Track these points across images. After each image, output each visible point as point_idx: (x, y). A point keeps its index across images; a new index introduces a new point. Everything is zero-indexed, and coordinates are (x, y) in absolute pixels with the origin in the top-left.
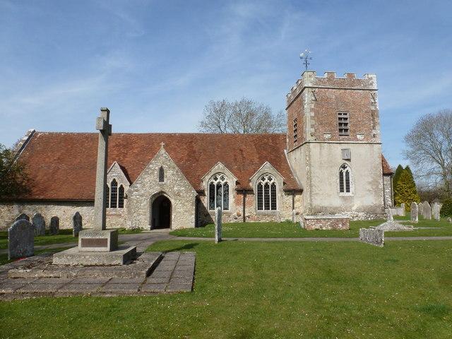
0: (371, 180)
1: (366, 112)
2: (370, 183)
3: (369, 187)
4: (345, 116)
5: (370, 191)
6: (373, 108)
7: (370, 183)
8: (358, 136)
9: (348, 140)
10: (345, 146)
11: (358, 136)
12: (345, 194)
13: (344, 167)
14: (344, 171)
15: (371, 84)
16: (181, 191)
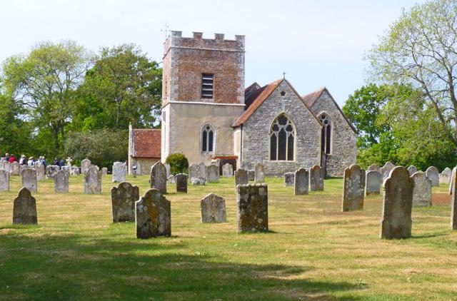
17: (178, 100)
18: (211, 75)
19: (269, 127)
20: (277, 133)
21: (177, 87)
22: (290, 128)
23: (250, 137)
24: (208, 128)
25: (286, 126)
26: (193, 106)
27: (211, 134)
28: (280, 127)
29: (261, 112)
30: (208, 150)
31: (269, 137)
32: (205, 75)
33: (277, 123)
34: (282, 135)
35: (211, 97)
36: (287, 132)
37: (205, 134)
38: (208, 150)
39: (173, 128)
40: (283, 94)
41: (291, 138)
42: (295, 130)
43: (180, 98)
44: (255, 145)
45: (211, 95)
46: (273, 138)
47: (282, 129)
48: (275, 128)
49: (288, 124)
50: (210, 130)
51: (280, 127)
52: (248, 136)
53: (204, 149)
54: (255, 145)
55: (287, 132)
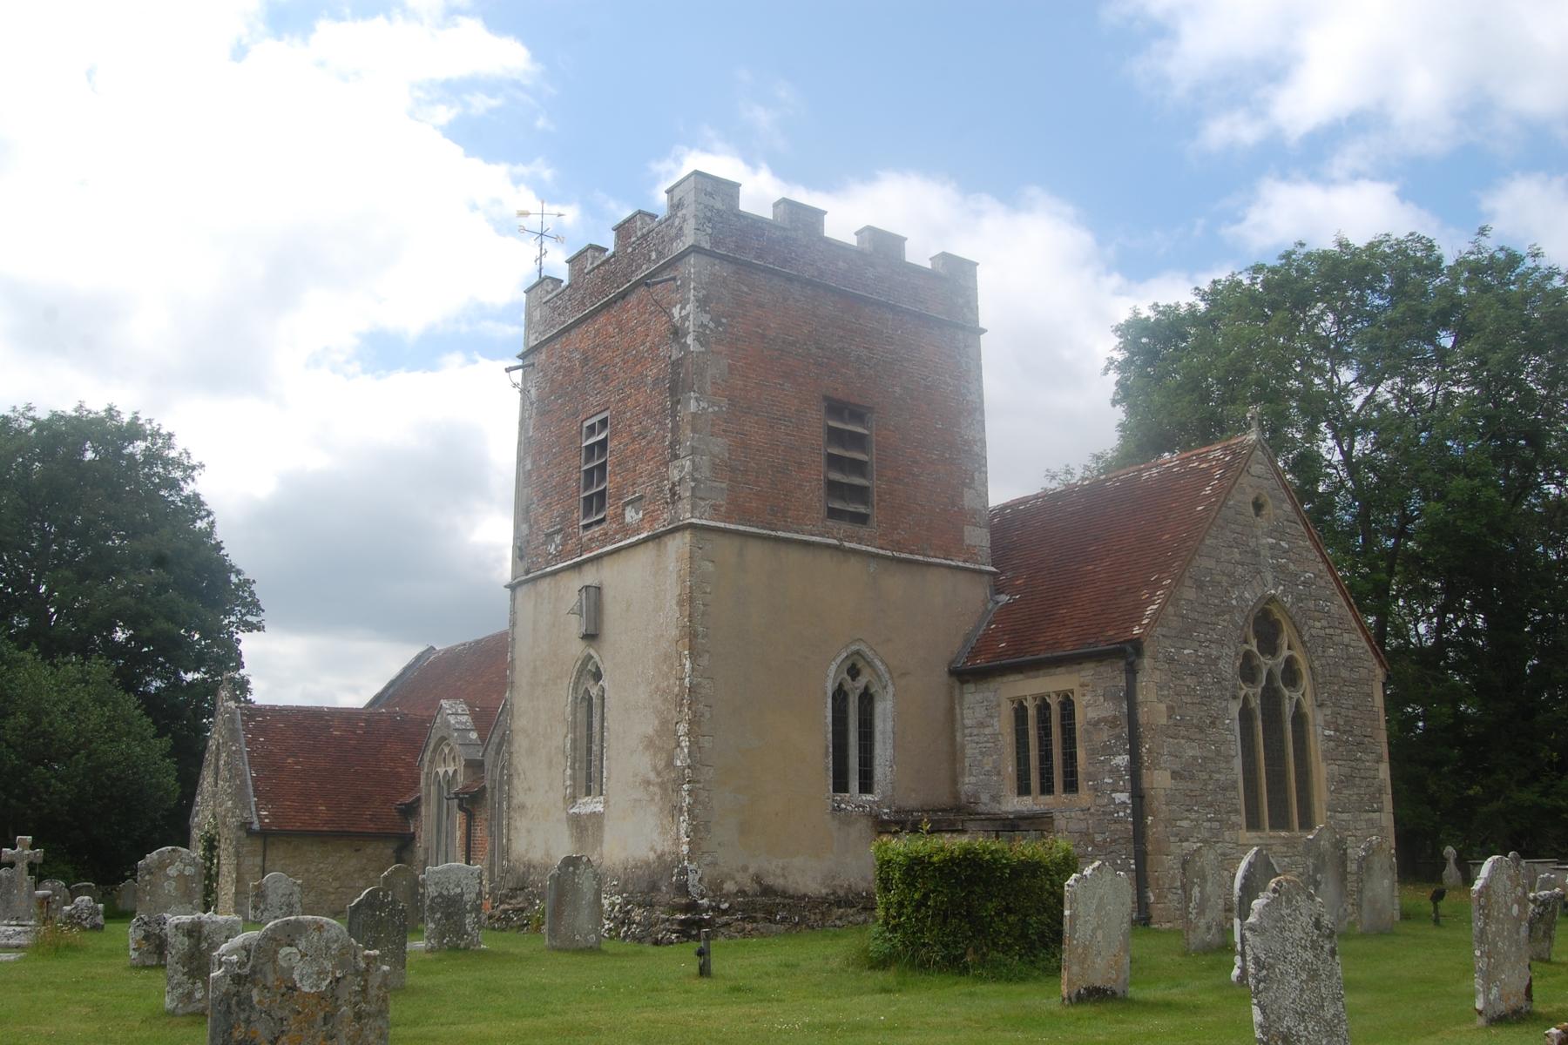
0: (647, 725)
1: (656, 382)
2: (650, 744)
3: (644, 764)
4: (602, 436)
5: (648, 783)
6: (676, 354)
7: (650, 744)
8: (631, 516)
9: (606, 538)
10: (590, 576)
11: (631, 516)
12: (590, 805)
13: (597, 676)
14: (594, 691)
15: (680, 233)
16: (227, 810)
17: (727, 519)
18: (858, 415)
19: (1229, 667)
20: (1254, 693)
21: (719, 446)
22: (1291, 674)
23: (1170, 708)
24: (854, 672)
25: (1281, 659)
26: (793, 556)
27: (867, 699)
28: (1265, 663)
29: (1200, 586)
30: (854, 784)
31: (1235, 708)
32: (836, 408)
33: (1253, 646)
34: (1271, 698)
35: (862, 519)
36: (1286, 692)
37: (840, 696)
38: (854, 784)
39: (704, 661)
40: (1258, 506)
41: (1300, 719)
42: (1306, 682)
43: (737, 510)
44: (1191, 751)
45: (862, 509)
46: (1246, 716)
47: (1270, 674)
48: (1248, 671)
49: (1285, 653)
50: (862, 681)
51: (1265, 663)
52: (1163, 707)
53: (840, 785)
54: (1191, 751)
55: (1286, 692)
